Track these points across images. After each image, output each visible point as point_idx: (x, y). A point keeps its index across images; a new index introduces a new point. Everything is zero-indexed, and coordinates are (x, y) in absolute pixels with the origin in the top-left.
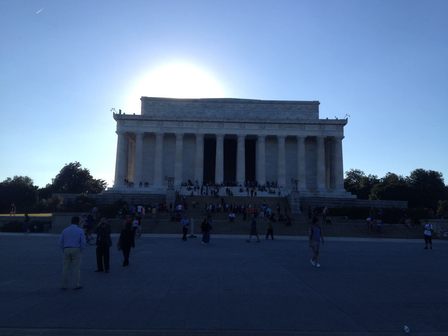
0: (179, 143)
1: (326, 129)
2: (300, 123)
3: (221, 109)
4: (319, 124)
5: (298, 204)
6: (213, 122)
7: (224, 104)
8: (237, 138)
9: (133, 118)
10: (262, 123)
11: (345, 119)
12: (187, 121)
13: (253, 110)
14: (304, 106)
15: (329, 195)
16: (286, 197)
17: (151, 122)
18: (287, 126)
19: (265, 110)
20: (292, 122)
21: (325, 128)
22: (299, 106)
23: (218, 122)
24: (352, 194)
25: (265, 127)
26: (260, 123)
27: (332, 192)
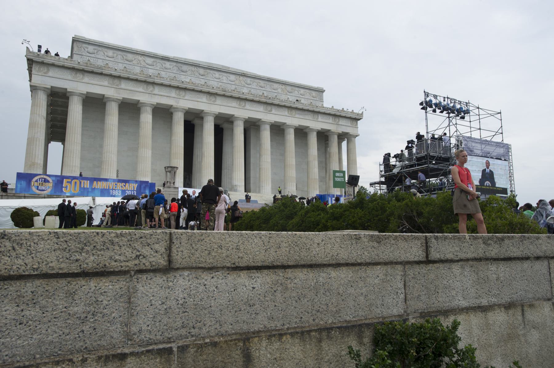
0: (147, 118)
1: (340, 123)
2: (313, 112)
3: (202, 77)
4: (335, 116)
6: (201, 92)
10: (268, 104)
11: (360, 112)
12: (162, 85)
13: (247, 86)
14: (307, 91)
17: (100, 77)
18: (298, 112)
19: (262, 89)
20: (305, 108)
22: (302, 91)
23: (209, 93)
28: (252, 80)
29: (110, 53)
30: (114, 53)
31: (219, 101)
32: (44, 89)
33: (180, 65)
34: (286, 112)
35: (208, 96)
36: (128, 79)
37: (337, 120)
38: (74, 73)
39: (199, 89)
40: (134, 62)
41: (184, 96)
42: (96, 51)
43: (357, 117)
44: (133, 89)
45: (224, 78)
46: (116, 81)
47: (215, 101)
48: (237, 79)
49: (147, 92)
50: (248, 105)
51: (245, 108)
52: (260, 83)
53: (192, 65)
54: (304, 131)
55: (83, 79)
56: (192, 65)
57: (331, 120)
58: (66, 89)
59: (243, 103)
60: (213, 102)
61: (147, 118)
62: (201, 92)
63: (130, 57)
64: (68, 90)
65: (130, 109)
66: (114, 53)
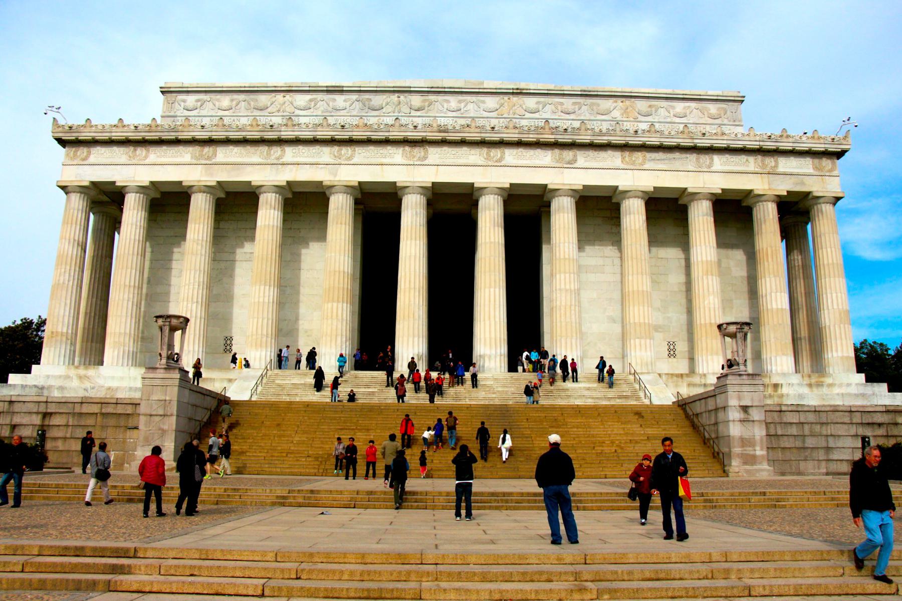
3: (418, 113)
5: (759, 432)
7: (432, 97)
8: (475, 204)
9: (117, 135)
13: (528, 115)
14: (693, 105)
15: (812, 399)
16: (683, 405)
19: (567, 117)
21: (776, 166)
22: (680, 106)
24: (890, 391)
25: (575, 161)
26: (555, 145)
27: (819, 385)
28: (542, 99)
29: (225, 101)
30: (232, 100)
31: (435, 154)
32: (83, 190)
33: (366, 96)
34: (614, 158)
35: (407, 148)
36: (227, 142)
37: (770, 161)
38: (132, 148)
39: (381, 135)
40: (269, 110)
41: (349, 159)
42: (199, 104)
43: (832, 148)
44: (239, 160)
45: (471, 106)
46: (207, 150)
47: (425, 158)
48: (502, 105)
49: (269, 161)
50: (511, 155)
51: (503, 163)
52: (562, 104)
53: (394, 92)
54: (680, 202)
55: (146, 157)
56: (394, 92)
57: (752, 163)
58: (114, 182)
59: (496, 153)
60: (419, 159)
61: (269, 216)
62: (387, 142)
63: (263, 99)
64: (117, 184)
65: (235, 205)
66: (232, 100)
